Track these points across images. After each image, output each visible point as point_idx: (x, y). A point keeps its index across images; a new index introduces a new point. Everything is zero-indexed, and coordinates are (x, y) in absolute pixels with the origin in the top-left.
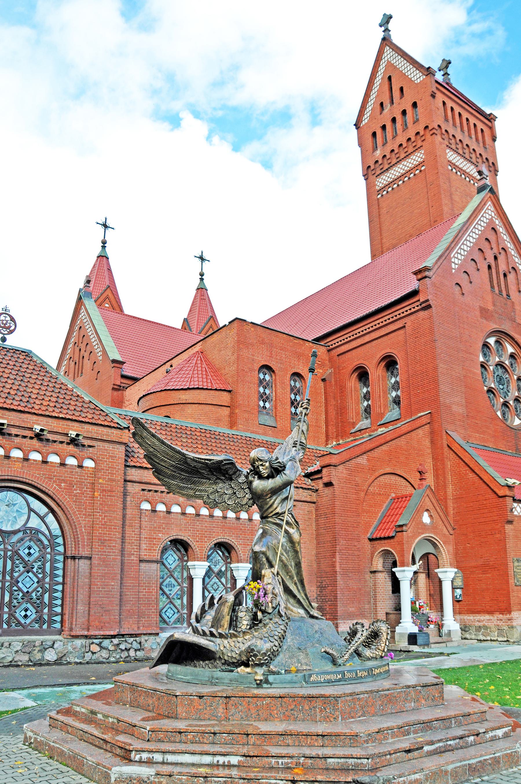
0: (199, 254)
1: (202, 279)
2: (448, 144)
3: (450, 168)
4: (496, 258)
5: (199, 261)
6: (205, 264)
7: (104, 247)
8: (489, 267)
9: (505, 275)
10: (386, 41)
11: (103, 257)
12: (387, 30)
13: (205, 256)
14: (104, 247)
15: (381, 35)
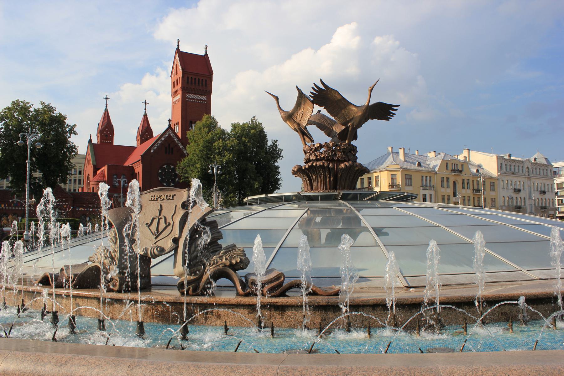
0: (144, 101)
1: (145, 111)
2: (187, 91)
3: (187, 100)
4: (169, 145)
5: (144, 104)
6: (147, 105)
7: (106, 107)
8: (166, 148)
9: (172, 149)
10: (178, 49)
11: (106, 111)
12: (178, 46)
13: (147, 102)
14: (106, 107)
15: (177, 47)
